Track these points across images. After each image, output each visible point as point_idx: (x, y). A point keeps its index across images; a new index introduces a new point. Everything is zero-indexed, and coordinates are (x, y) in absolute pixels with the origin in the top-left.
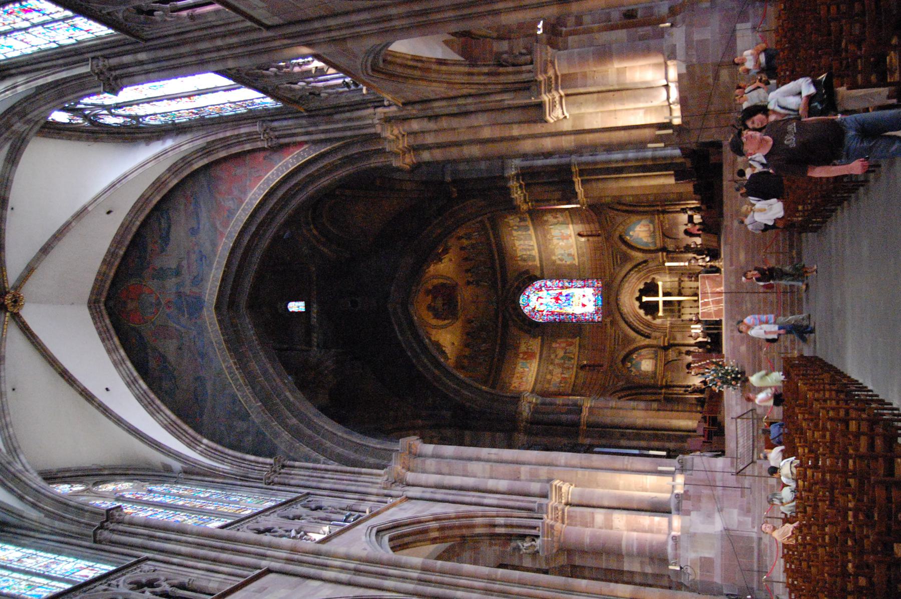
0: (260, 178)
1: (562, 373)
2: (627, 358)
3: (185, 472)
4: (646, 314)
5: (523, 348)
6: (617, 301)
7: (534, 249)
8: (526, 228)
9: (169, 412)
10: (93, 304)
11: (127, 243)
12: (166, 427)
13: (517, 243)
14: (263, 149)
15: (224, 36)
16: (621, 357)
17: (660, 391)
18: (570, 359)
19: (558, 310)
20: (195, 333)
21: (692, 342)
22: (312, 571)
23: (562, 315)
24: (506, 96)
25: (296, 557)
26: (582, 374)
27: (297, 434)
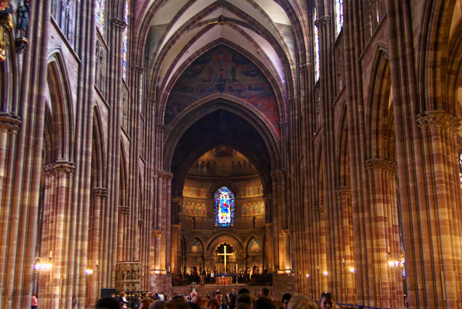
0: (269, 118)
1: (191, 210)
2: (198, 239)
3: (158, 87)
4: (218, 248)
5: (202, 190)
9: (179, 76)
10: (221, 40)
11: (246, 57)
12: (173, 77)
13: (252, 188)
14: (279, 121)
15: (299, 148)
16: (198, 237)
17: (184, 255)
18: (197, 213)
19: (220, 206)
20: (210, 88)
21: (205, 269)
22: (146, 178)
24: (290, 216)
27: (173, 132)
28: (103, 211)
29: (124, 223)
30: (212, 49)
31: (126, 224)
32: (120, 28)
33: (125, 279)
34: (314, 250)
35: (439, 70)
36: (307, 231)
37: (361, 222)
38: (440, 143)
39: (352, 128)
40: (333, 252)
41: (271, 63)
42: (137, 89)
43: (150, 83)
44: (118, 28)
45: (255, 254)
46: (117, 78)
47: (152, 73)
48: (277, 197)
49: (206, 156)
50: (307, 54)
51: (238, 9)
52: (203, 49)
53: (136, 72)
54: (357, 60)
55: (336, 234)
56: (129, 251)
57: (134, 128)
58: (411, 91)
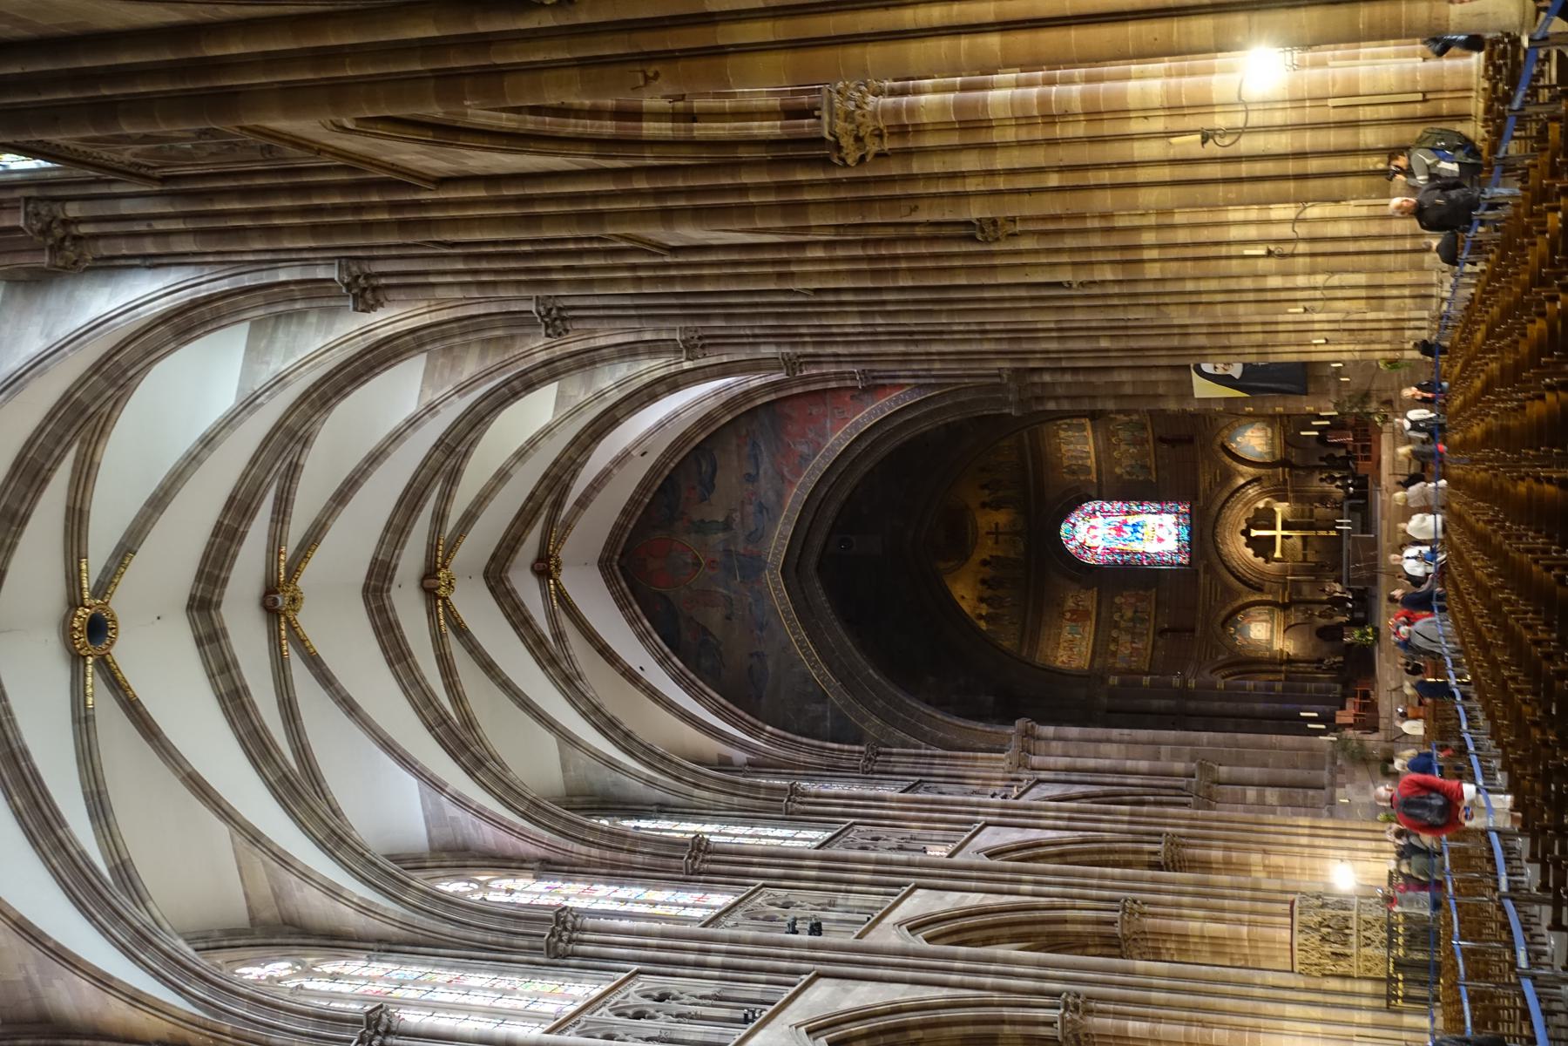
0: (846, 420)
2: (1230, 618)
3: (750, 764)
4: (1256, 555)
5: (1070, 603)
6: (1214, 535)
7: (1089, 457)
8: (1082, 428)
9: (716, 696)
10: (604, 565)
11: (655, 488)
12: (717, 714)
13: (1064, 448)
16: (1220, 619)
18: (1143, 621)
19: (1121, 547)
20: (750, 600)
21: (1325, 598)
22: (1030, 821)
23: (1127, 554)
25: (1010, 811)
26: (1160, 643)
28: (1131, 1009)
29: (1169, 916)
30: (634, 596)
31: (1174, 911)
32: (574, 929)
33: (1347, 951)
34: (1264, 323)
35: (698, 104)
36: (1202, 341)
37: (1174, 253)
38: (923, 98)
39: (875, 273)
40: (1269, 296)
41: (676, 414)
42: (755, 860)
43: (736, 800)
44: (575, 935)
45: (1277, 441)
46: (723, 947)
47: (706, 794)
48: (1094, 397)
49: (965, 593)
50: (648, 336)
51: (512, 525)
52: (632, 621)
53: (703, 861)
54: (668, 259)
55: (1213, 285)
56: (1260, 906)
57: (875, 872)
58: (765, 178)
